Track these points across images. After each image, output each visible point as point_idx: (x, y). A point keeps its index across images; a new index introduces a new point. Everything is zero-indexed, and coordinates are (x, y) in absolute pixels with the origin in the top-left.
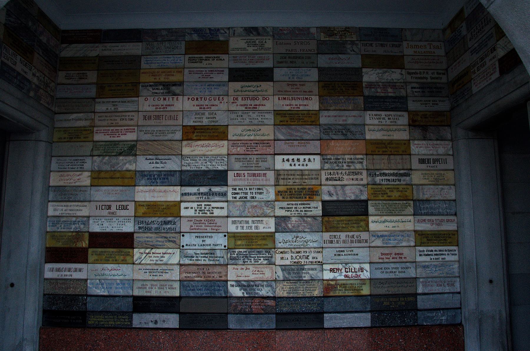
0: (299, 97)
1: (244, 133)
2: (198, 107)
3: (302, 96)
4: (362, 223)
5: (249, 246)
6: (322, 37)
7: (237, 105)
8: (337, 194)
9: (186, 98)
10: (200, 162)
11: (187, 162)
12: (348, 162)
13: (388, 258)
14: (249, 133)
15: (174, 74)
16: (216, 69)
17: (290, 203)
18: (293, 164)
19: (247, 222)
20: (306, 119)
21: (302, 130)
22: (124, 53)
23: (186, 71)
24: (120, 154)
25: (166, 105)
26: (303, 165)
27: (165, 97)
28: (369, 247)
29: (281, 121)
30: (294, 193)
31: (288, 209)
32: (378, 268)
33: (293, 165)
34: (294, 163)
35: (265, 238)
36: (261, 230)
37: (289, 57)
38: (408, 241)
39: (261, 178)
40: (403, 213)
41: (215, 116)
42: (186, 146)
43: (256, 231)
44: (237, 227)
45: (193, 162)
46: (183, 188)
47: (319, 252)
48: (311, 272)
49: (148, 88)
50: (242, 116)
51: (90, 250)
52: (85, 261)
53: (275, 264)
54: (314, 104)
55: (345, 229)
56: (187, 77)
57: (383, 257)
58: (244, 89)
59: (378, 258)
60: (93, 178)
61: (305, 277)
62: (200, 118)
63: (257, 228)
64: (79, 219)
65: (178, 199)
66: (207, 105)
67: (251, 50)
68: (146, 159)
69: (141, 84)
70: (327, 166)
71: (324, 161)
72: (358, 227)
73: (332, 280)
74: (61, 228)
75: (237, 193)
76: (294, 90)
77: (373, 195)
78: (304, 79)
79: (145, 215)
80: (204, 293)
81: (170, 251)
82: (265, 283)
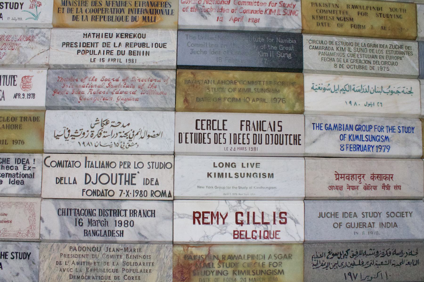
4: (287, 92)
13: (354, 188)
17: (92, 31)
28: (305, 156)
30: (104, 6)
31: (85, 48)
32: (326, 215)
35: (18, 122)
38: (406, 143)
40: (393, 70)
47: (165, 166)
48: (138, 220)
53: (39, 196)
55: (238, 106)
57: (342, 182)
59: (326, 186)
61: (122, 234)
73: (199, 245)
77: (315, 22)
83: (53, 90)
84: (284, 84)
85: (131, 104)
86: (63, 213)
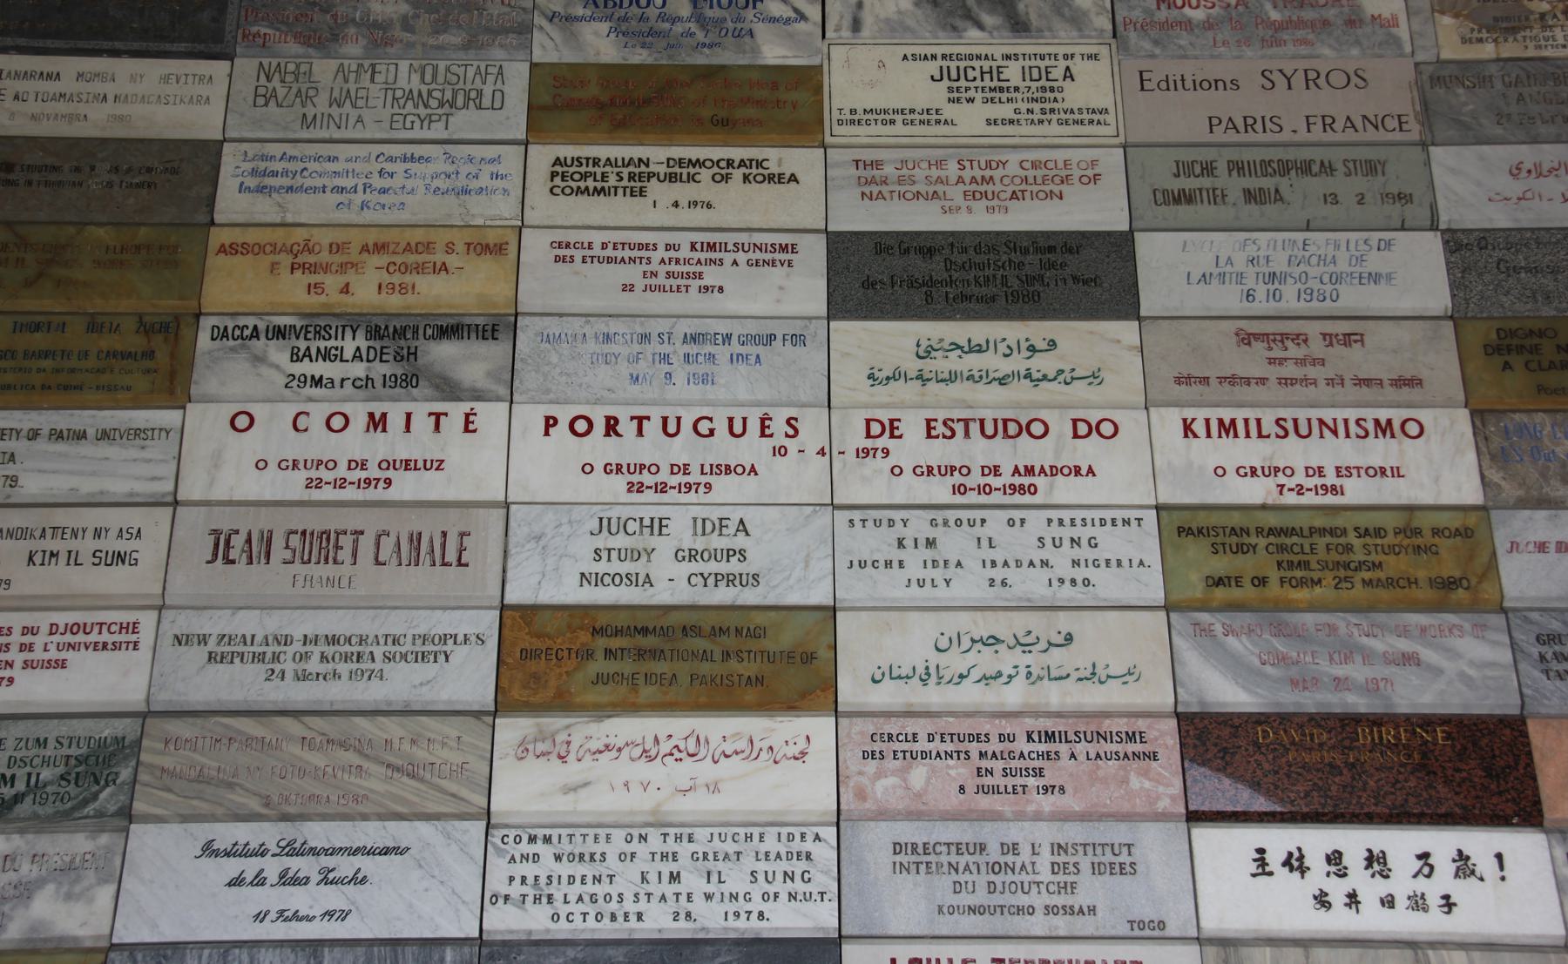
0: (1328, 415)
1: (955, 662)
2: (620, 482)
3: (1352, 414)
7: (897, 471)
9: (530, 416)
10: (632, 871)
11: (529, 870)
14: (985, 660)
15: (453, 261)
16: (743, 238)
18: (1337, 890)
20: (1395, 565)
21: (1378, 645)
22: (96, 122)
23: (536, 246)
25: (391, 465)
26: (1418, 903)
27: (378, 408)
29: (1219, 582)
33: (1337, 896)
34: (1344, 886)
37: (1236, 167)
41: (740, 541)
42: (523, 750)
45: (579, 869)
49: (259, 345)
50: (931, 543)
54: (1438, 467)
56: (542, 283)
58: (941, 364)
62: (635, 555)
66: (685, 469)
67: (971, 119)
68: (209, 850)
69: (207, 323)
76: (1290, 370)
78: (1353, 298)
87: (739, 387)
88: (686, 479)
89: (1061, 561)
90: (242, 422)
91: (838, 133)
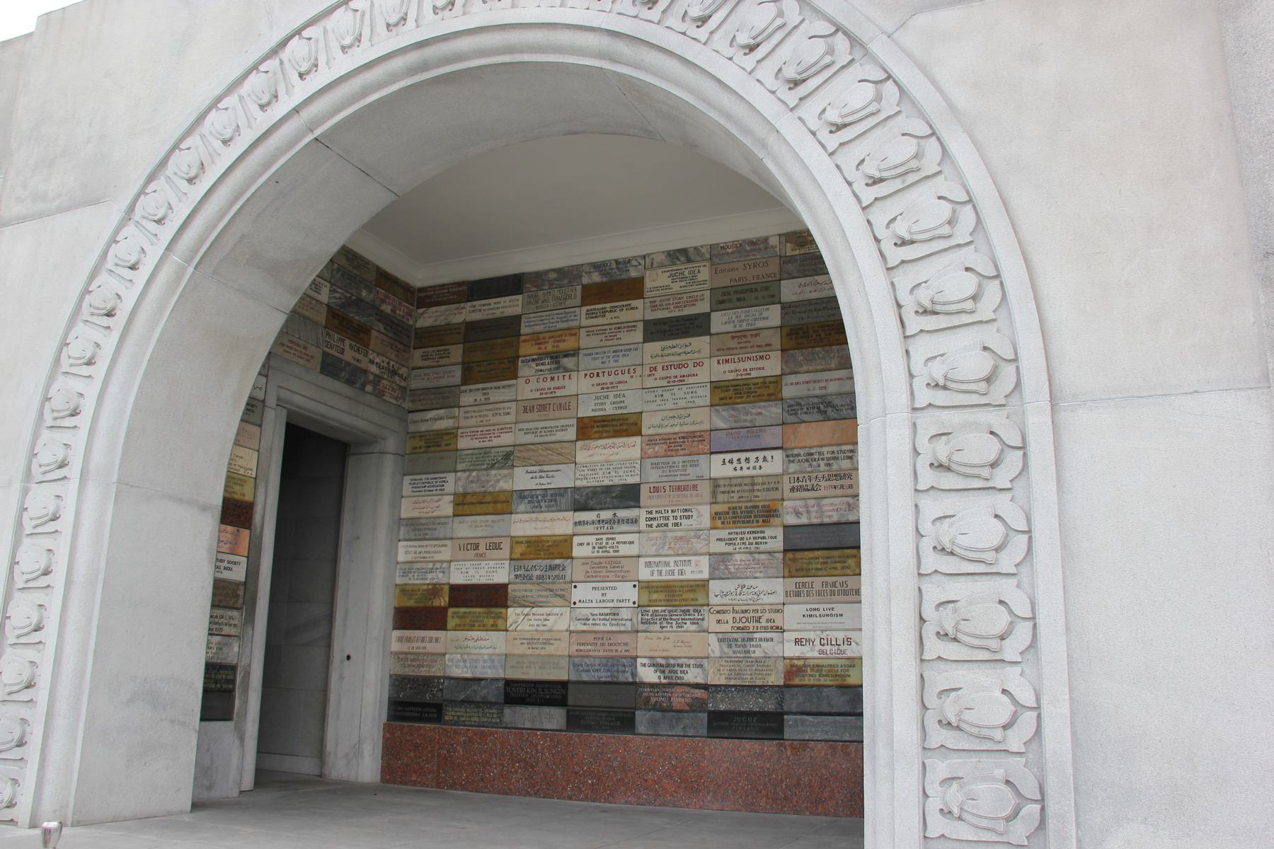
1: (665, 423)
4: (851, 562)
5: (669, 602)
6: (790, 250)
8: (808, 512)
9: (582, 374)
12: (828, 459)
14: (671, 422)
19: (667, 564)
20: (760, 391)
22: (498, 313)
24: (492, 466)
26: (754, 468)
31: (730, 542)
36: (688, 576)
37: (735, 292)
39: (688, 493)
42: (581, 448)
43: (681, 577)
44: (652, 574)
46: (577, 514)
48: (763, 644)
51: (451, 611)
52: (443, 627)
54: (772, 366)
55: (821, 573)
56: (585, 341)
58: (666, 352)
60: (456, 504)
63: (681, 572)
64: (438, 565)
65: (570, 532)
70: (793, 467)
71: (790, 458)
72: (843, 568)
73: (799, 658)
74: (414, 580)
75: (654, 519)
78: (759, 324)
79: (523, 556)
80: (603, 676)
81: (556, 610)
82: (692, 662)
83: (713, 568)
84: (848, 557)
85: (758, 575)
86: (720, 640)
87: (624, 361)
88: (613, 386)
89: (689, 397)
90: (527, 382)
91: (647, 294)
